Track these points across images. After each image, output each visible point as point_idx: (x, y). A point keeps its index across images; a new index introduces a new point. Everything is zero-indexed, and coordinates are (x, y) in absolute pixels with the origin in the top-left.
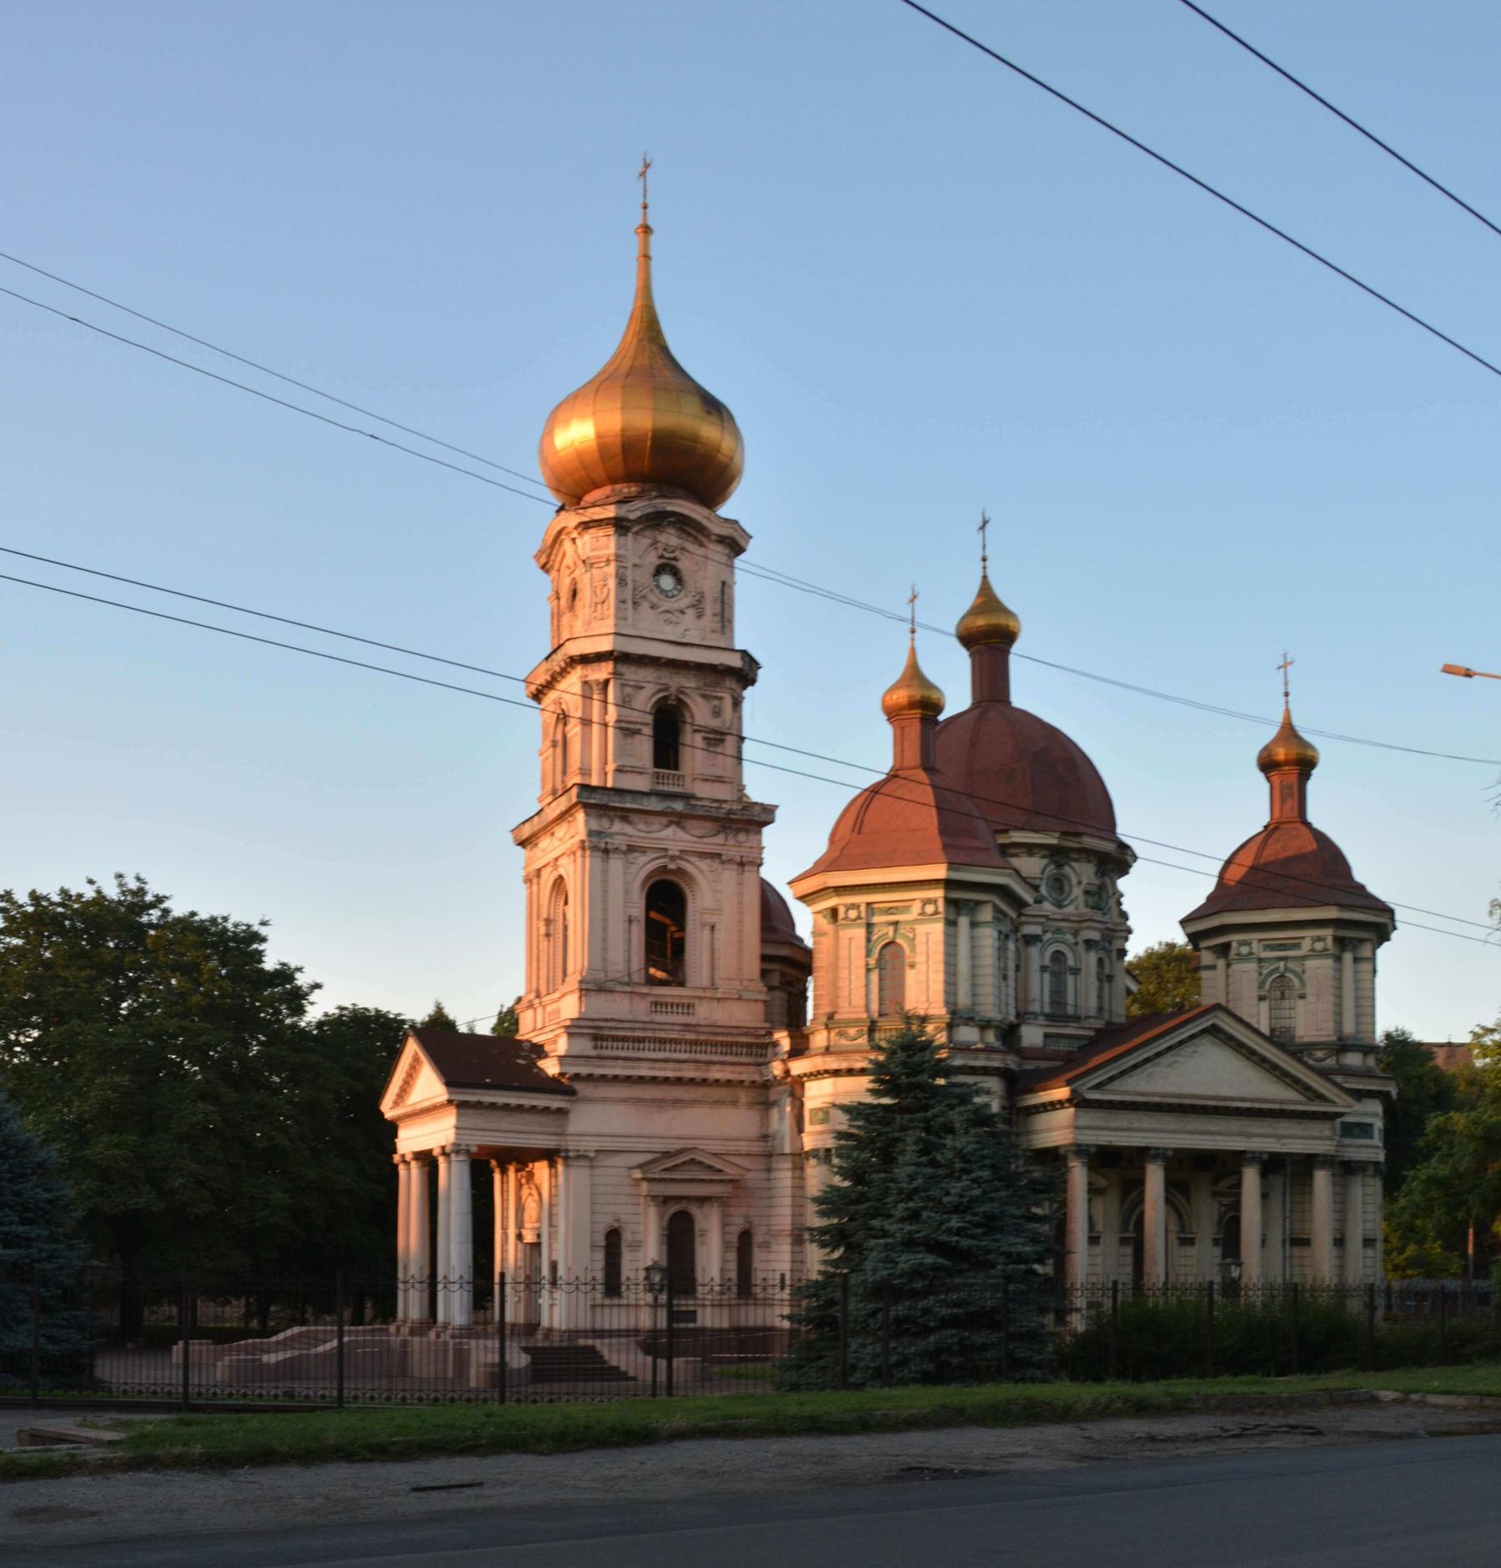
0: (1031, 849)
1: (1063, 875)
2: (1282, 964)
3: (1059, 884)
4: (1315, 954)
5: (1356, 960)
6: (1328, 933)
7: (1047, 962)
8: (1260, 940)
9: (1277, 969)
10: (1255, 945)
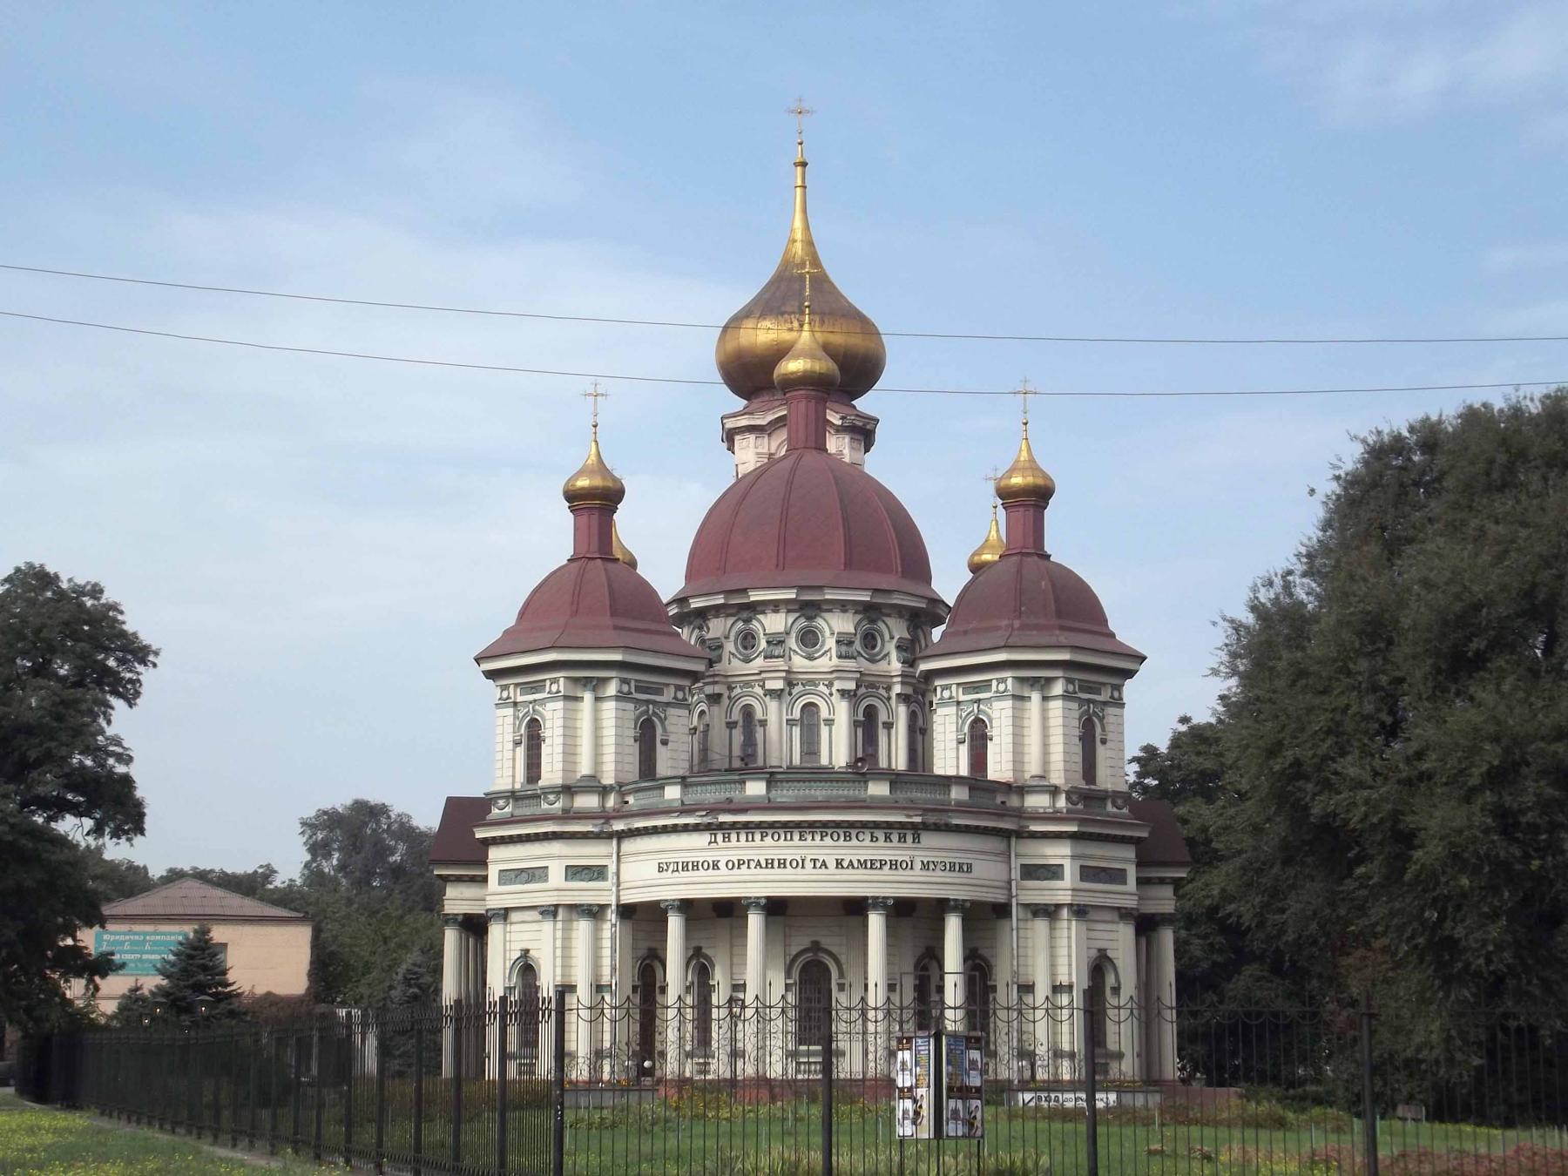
0: (775, 606)
1: (817, 628)
2: (976, 705)
3: (809, 639)
4: (1001, 696)
5: (1045, 699)
6: (1008, 674)
7: (797, 714)
8: (958, 684)
9: (973, 711)
10: (954, 687)
